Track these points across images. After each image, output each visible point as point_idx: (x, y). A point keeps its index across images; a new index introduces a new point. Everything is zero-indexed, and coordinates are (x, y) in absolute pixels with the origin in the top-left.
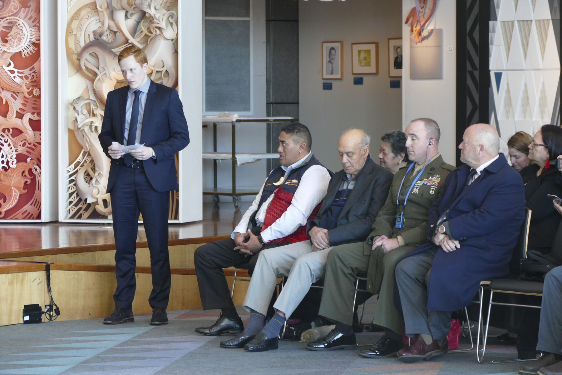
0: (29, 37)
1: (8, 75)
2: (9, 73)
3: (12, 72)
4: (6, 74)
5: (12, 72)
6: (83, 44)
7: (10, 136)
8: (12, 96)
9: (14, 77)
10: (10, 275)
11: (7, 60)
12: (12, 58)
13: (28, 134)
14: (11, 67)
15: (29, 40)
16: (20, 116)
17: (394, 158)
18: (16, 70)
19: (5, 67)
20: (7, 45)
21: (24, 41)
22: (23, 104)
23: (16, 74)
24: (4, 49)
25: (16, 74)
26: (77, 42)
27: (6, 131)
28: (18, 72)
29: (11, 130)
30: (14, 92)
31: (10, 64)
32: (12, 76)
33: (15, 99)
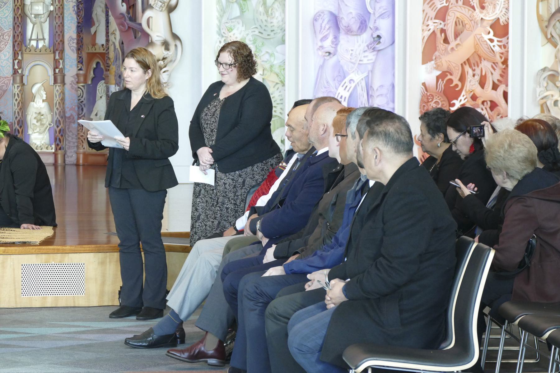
0: (503, 3)
1: (487, 44)
2: (489, 42)
3: (492, 41)
4: (485, 43)
5: (492, 41)
6: (553, 10)
7: (488, 109)
8: (492, 67)
9: (494, 46)
10: (100, 255)
11: (485, 27)
12: (491, 27)
13: (502, 107)
14: (491, 36)
15: (502, 6)
16: (495, 87)
17: (431, 139)
18: (496, 39)
19: (483, 35)
20: (484, 11)
21: (498, 7)
22: (501, 76)
23: (496, 43)
24: (482, 16)
25: (496, 43)
26: (549, 8)
27: (485, 103)
28: (498, 41)
29: (489, 103)
30: (494, 63)
31: (489, 33)
32: (492, 45)
33: (494, 69)
